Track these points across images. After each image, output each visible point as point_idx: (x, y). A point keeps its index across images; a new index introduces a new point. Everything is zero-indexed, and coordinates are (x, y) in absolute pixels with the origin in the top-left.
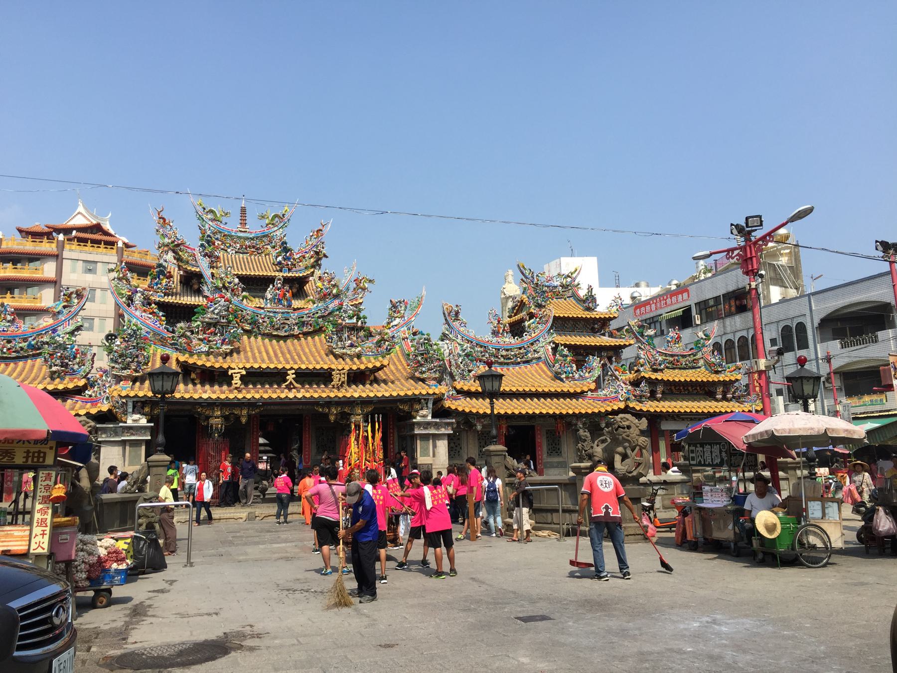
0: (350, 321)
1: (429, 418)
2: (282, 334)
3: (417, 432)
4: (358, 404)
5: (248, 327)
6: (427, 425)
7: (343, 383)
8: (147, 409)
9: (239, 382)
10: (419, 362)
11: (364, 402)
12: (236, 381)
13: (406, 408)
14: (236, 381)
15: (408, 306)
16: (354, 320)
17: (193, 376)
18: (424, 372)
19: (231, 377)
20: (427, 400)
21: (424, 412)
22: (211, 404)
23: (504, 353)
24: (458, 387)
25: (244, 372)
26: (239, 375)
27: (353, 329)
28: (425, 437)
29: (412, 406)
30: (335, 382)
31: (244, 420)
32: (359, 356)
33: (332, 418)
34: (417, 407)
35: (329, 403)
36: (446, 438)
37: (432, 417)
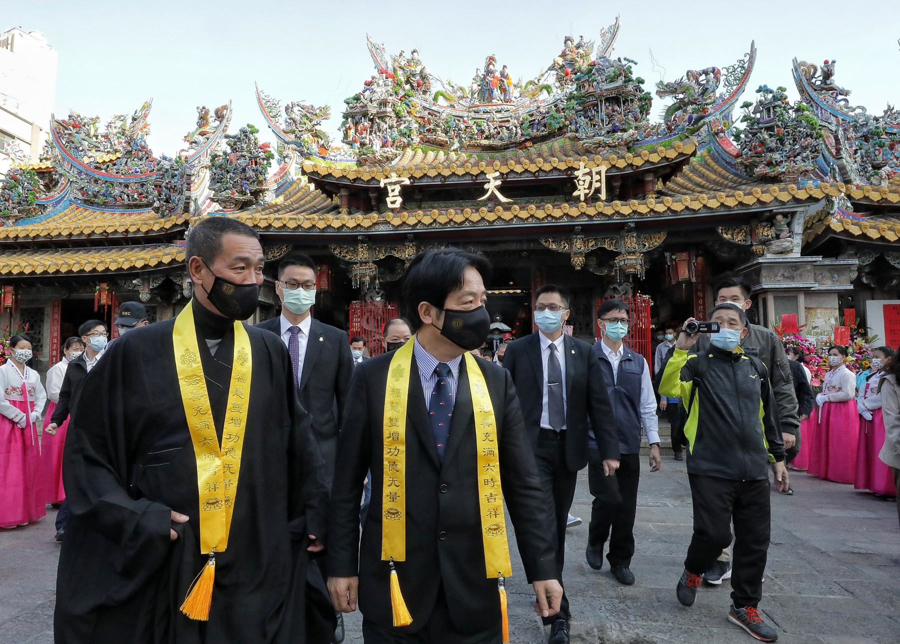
0: (612, 85)
1: (796, 255)
2: (496, 142)
4: (630, 230)
5: (442, 137)
6: (794, 266)
7: (598, 191)
9: (399, 200)
10: (762, 143)
11: (644, 227)
12: (394, 199)
13: (739, 238)
14: (394, 199)
15: (722, 78)
16: (620, 82)
18: (778, 164)
19: (383, 193)
20: (790, 216)
22: (351, 240)
24: (857, 195)
25: (407, 182)
26: (398, 188)
27: (614, 100)
28: (788, 296)
29: (752, 233)
30: (581, 192)
32: (630, 146)
33: (578, 262)
34: (766, 232)
36: (835, 302)
37: (804, 253)
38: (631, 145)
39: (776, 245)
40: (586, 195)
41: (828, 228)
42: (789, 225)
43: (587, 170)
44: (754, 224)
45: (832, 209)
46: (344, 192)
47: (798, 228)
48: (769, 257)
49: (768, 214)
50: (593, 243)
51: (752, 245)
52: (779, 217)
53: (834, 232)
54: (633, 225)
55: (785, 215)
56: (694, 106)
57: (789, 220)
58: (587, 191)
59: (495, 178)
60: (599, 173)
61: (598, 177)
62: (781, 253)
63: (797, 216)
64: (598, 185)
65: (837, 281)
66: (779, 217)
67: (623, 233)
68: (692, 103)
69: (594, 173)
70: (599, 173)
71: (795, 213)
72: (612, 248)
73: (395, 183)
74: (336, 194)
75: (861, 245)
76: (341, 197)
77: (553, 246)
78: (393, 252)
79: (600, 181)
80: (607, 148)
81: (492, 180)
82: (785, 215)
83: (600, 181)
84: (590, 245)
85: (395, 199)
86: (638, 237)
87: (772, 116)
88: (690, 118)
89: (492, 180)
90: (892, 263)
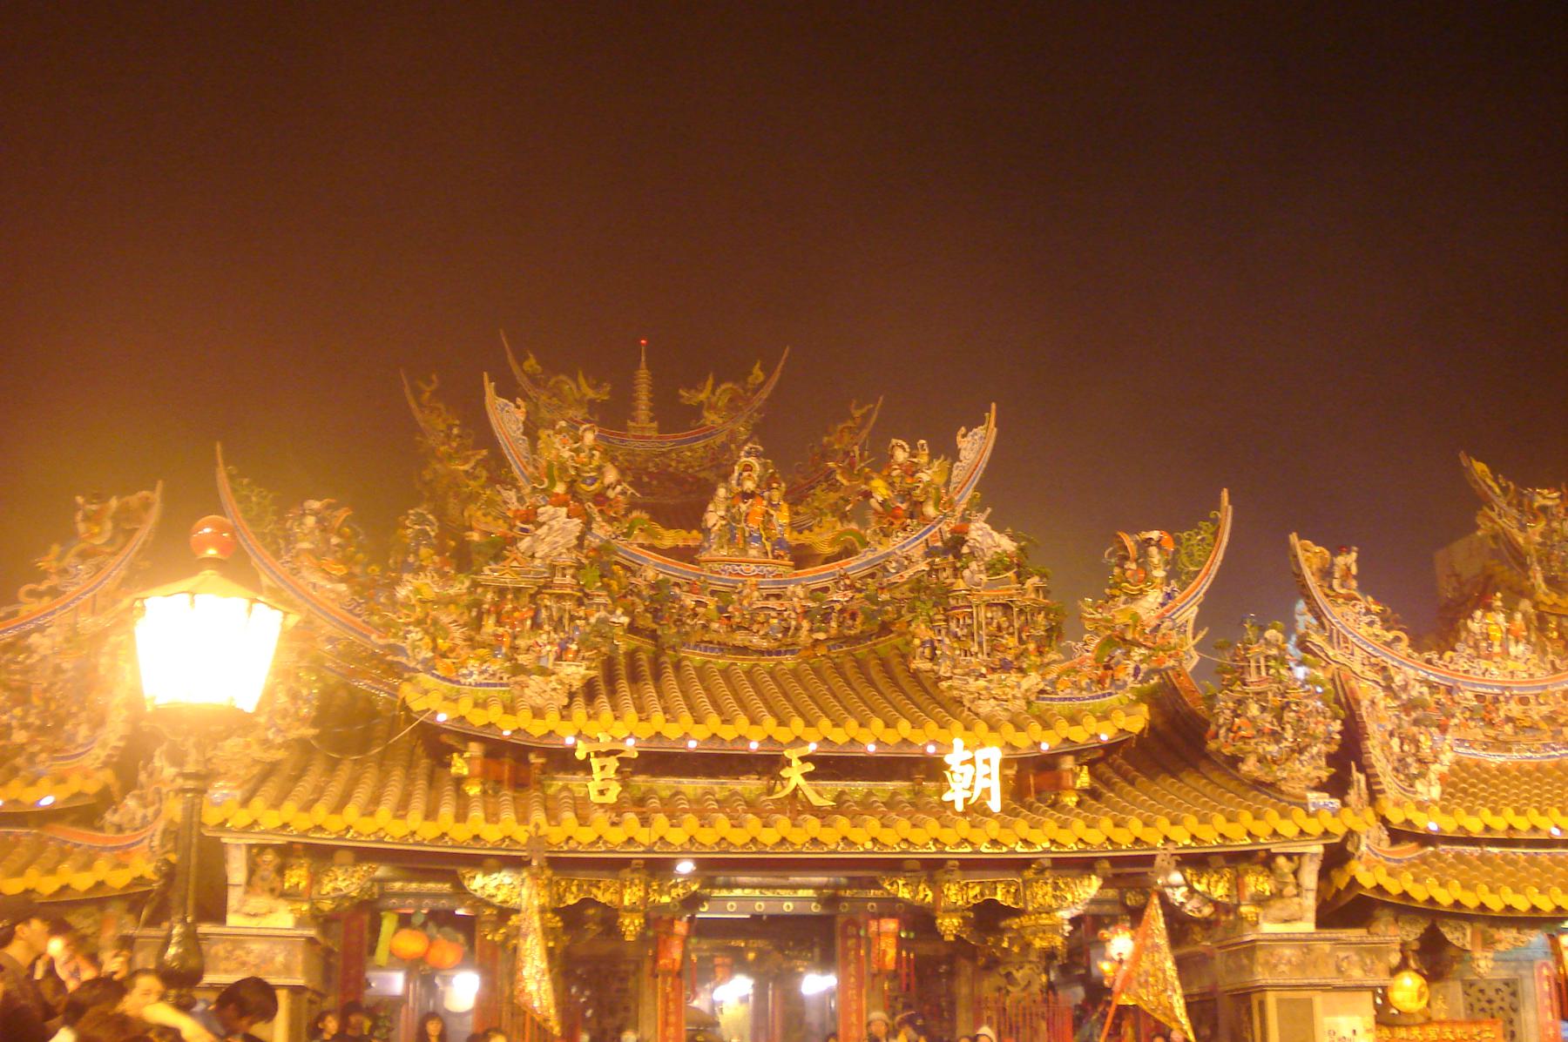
1: (1307, 926)
3: (1262, 976)
8: (297, 877)
17: (459, 766)
21: (1293, 906)
23: (1515, 709)
26: (613, 763)
29: (1237, 885)
30: (956, 794)
31: (631, 925)
33: (949, 925)
35: (932, 869)
38: (1033, 698)
39: (1277, 908)
40: (966, 800)
41: (1353, 879)
42: (1295, 873)
43: (968, 755)
44: (1242, 867)
45: (1357, 848)
46: (475, 749)
47: (1310, 878)
48: (1268, 928)
49: (1263, 854)
50: (977, 889)
51: (1239, 905)
52: (1281, 861)
53: (1362, 887)
54: (1048, 863)
55: (1289, 856)
56: (1143, 651)
57: (1292, 866)
58: (968, 794)
59: (804, 759)
60: (987, 762)
61: (982, 769)
62: (1286, 921)
63: (1306, 860)
64: (985, 783)
65: (1370, 971)
66: (1281, 861)
67: (1029, 874)
68: (1139, 645)
69: (979, 761)
70: (987, 762)
71: (1301, 855)
72: (1009, 902)
73: (609, 753)
74: (461, 753)
75: (1404, 908)
76: (468, 761)
77: (904, 893)
78: (594, 890)
79: (988, 776)
80: (992, 702)
81: (796, 763)
82: (1289, 856)
83: (988, 776)
84: (972, 893)
85: (601, 786)
86: (1056, 887)
87: (1264, 673)
88: (1137, 670)
89: (796, 763)
90: (1449, 937)
